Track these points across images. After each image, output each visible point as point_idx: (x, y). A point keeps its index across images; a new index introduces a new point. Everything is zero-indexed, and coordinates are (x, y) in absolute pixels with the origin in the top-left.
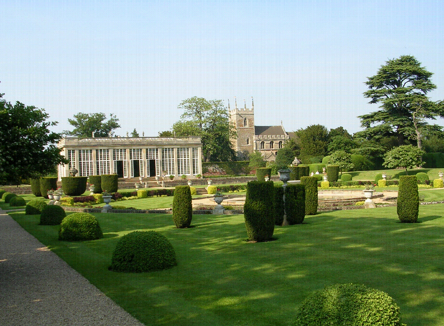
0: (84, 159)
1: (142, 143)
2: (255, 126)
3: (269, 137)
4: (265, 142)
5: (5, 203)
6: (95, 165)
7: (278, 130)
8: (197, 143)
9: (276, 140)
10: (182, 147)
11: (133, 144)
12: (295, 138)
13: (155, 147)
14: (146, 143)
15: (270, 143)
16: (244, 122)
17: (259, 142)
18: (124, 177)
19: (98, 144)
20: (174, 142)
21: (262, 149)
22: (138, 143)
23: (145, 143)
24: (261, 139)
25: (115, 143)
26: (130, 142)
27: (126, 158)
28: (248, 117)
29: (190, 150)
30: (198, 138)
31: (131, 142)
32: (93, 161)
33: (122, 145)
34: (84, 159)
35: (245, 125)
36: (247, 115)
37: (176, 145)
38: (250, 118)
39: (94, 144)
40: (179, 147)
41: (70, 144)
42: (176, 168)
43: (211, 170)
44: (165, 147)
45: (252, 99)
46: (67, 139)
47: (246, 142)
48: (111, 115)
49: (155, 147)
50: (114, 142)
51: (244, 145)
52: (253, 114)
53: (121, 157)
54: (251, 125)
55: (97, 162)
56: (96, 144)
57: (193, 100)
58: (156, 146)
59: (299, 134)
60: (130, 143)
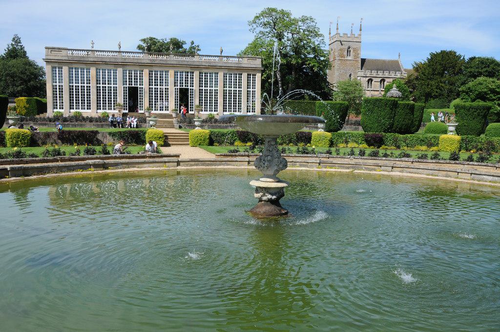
2: (361, 59)
3: (379, 73)
4: (374, 80)
6: (93, 91)
7: (394, 66)
9: (389, 78)
11: (154, 62)
12: (413, 72)
13: (189, 70)
14: (175, 63)
15: (381, 82)
16: (346, 52)
17: (364, 78)
18: (140, 112)
21: (368, 89)
23: (172, 63)
25: (127, 61)
27: (144, 83)
28: (353, 45)
29: (244, 76)
38: (355, 47)
39: (92, 60)
40: (226, 72)
41: (54, 58)
42: (221, 101)
44: (204, 71)
48: (193, 43)
50: (125, 59)
54: (357, 55)
55: (97, 87)
57: (270, 11)
59: (418, 68)
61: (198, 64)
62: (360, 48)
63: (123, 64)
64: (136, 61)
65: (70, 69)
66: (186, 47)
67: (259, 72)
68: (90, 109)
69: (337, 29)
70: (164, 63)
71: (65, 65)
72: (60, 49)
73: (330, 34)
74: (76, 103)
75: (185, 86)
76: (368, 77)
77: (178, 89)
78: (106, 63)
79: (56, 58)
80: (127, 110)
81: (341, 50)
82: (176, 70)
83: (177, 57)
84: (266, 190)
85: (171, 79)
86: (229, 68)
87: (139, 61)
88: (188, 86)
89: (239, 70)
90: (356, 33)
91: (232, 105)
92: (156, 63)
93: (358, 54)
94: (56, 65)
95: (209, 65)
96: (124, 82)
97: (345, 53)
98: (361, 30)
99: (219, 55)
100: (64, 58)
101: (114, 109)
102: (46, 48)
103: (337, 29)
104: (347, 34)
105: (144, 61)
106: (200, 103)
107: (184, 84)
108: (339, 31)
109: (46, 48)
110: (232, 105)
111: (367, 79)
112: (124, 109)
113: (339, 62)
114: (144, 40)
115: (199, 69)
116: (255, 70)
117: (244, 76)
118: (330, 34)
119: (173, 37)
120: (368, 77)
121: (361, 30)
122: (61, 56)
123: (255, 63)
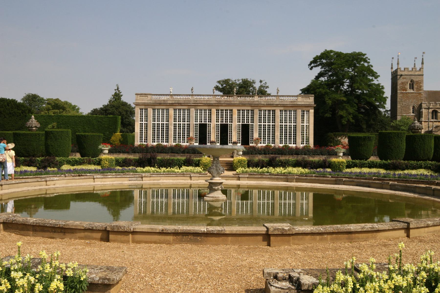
0: (184, 120)
1: (232, 103)
2: (425, 91)
5: (101, 165)
6: (171, 128)
8: (308, 104)
10: (286, 109)
14: (238, 103)
19: (176, 102)
20: (276, 101)
21: (432, 120)
22: (226, 102)
23: (236, 103)
24: (430, 107)
25: (198, 102)
26: (216, 101)
28: (415, 79)
29: (299, 112)
30: (310, 97)
31: (218, 101)
32: (152, 122)
33: (205, 105)
34: (184, 120)
35: (410, 88)
36: (413, 76)
37: (277, 106)
38: (417, 80)
39: (171, 102)
40: (282, 108)
43: (345, 143)
44: (263, 108)
45: (423, 56)
46: (139, 96)
47: (411, 111)
49: (249, 108)
50: (197, 101)
51: (407, 114)
52: (423, 75)
53: (226, 120)
54: (420, 88)
56: (173, 102)
58: (251, 106)
60: (217, 103)
61: (257, 103)
62: (422, 81)
63: (196, 105)
64: (205, 102)
65: (154, 110)
66: (257, 86)
67: (312, 109)
68: (168, 142)
69: (398, 64)
70: (228, 103)
71: (149, 108)
72: (146, 95)
73: (392, 68)
74: (157, 137)
75: (247, 122)
76: (431, 108)
77: (240, 124)
78: (180, 104)
79: (143, 102)
80: (197, 142)
81: (402, 83)
82: (239, 108)
83: (243, 98)
84: (208, 197)
85: (235, 116)
86: (284, 106)
87: (208, 102)
88: (249, 122)
89: (295, 107)
90: (418, 66)
91: (288, 138)
92: (222, 103)
93: (421, 87)
94: (143, 107)
95: (267, 103)
96: (196, 120)
97: (408, 86)
98: (422, 63)
99: (276, 94)
100: (149, 102)
101: (187, 142)
102: (136, 94)
103: (398, 64)
104: (408, 69)
105: (212, 102)
106: (259, 136)
107: (245, 121)
108: (400, 67)
109: (136, 94)
110: (288, 138)
111: (431, 110)
112: (195, 142)
113: (401, 95)
114: (219, 82)
115: (258, 107)
116: (308, 106)
117: (299, 112)
118: (392, 68)
119: (244, 78)
120: (431, 108)
121: (422, 63)
122: (146, 100)
123: (308, 101)
